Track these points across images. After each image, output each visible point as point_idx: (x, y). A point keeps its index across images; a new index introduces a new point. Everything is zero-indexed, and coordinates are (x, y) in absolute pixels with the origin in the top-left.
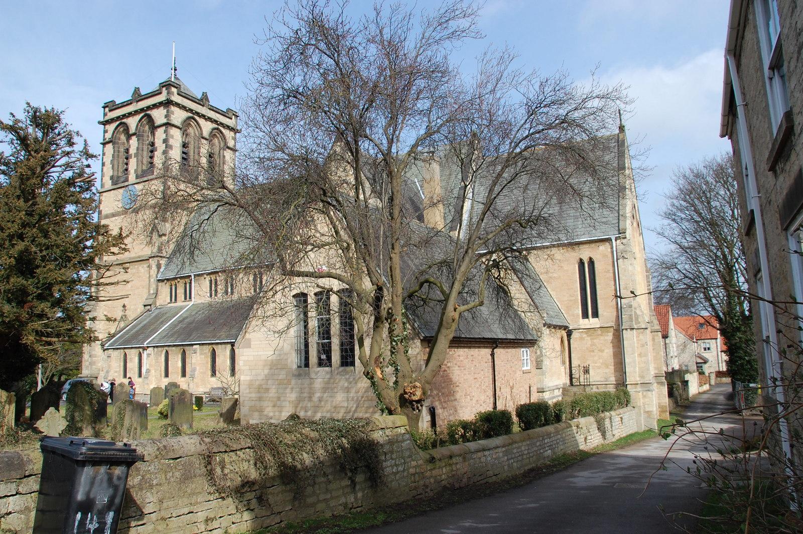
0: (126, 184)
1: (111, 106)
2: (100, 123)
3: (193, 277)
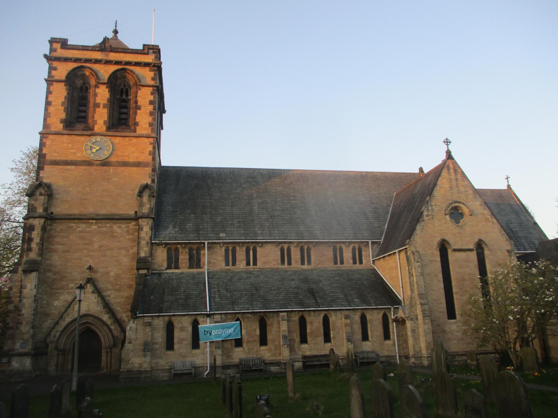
0: (89, 132)
1: (64, 43)
2: (45, 56)
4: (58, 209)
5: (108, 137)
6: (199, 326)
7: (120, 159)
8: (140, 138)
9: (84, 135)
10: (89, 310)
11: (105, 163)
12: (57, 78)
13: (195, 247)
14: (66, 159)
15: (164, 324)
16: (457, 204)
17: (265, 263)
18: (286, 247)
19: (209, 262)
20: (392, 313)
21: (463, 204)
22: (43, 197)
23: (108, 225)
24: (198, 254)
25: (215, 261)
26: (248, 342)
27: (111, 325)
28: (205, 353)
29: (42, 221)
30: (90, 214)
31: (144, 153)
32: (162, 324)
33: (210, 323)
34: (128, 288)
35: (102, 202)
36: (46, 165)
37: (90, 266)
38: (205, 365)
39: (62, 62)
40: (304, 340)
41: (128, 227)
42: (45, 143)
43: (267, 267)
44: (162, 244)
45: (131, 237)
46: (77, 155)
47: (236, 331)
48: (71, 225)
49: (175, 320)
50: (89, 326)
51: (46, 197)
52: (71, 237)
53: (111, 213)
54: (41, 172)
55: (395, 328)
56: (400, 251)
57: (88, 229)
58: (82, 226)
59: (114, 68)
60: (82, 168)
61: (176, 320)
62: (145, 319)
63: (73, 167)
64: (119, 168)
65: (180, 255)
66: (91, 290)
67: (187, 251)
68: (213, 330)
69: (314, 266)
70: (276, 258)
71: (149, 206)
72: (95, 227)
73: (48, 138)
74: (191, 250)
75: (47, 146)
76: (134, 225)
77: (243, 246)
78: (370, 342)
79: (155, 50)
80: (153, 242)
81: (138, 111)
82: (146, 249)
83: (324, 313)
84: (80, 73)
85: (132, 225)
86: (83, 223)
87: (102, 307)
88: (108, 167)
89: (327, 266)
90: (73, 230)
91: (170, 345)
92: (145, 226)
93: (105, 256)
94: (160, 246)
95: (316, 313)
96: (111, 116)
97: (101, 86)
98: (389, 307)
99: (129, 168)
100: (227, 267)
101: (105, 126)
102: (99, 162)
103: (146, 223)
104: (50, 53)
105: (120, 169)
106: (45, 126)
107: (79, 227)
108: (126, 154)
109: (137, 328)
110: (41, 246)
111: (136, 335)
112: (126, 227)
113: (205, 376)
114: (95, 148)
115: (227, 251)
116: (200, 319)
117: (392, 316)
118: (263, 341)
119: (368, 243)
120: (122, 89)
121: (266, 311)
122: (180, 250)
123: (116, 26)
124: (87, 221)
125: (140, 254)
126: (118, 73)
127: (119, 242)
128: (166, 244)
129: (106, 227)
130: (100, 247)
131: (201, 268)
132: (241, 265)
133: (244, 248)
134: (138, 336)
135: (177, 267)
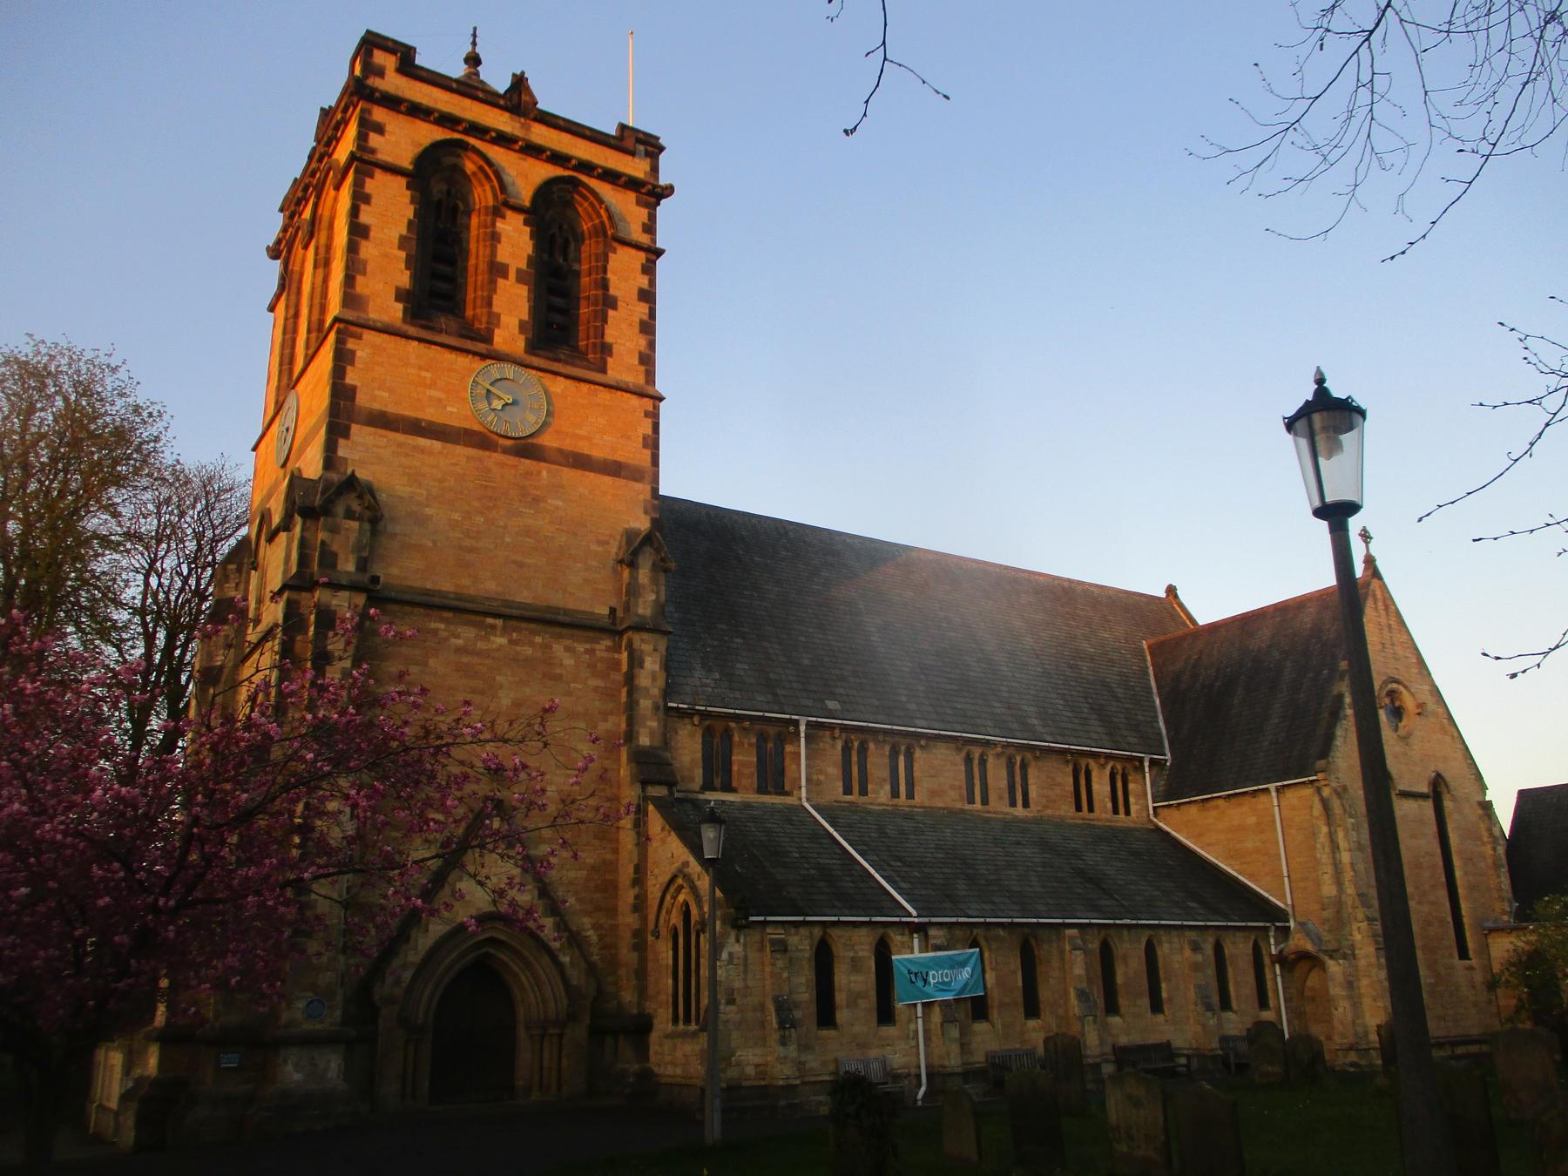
0: (481, 347)
3: (802, 728)
4: (395, 571)
5: (534, 372)
6: (894, 957)
7: (568, 445)
8: (619, 393)
9: (468, 352)
11: (526, 449)
13: (772, 731)
14: (415, 415)
15: (811, 949)
16: (1394, 686)
17: (933, 793)
18: (977, 752)
19: (808, 780)
20: (1272, 941)
21: (1406, 687)
22: (355, 525)
23: (538, 639)
24: (781, 754)
25: (822, 778)
27: (560, 950)
28: (911, 1035)
29: (361, 600)
30: (488, 599)
31: (629, 438)
32: (808, 948)
33: (921, 952)
34: (595, 838)
35: (521, 565)
36: (357, 423)
38: (913, 1071)
39: (399, 112)
40: (1112, 1007)
42: (353, 353)
43: (940, 805)
44: (694, 714)
45: (599, 683)
46: (449, 409)
47: (975, 977)
48: (433, 625)
49: (838, 938)
50: (492, 951)
51: (367, 526)
52: (431, 662)
53: (545, 604)
54: (341, 442)
55: (1279, 979)
56: (1284, 786)
57: (480, 645)
58: (466, 634)
60: (461, 450)
61: (840, 937)
62: (769, 930)
63: (437, 445)
64: (565, 469)
65: (735, 751)
67: (754, 740)
68: (933, 969)
69: (1038, 811)
70: (957, 783)
71: (653, 597)
72: (501, 641)
73: (360, 338)
74: (763, 738)
75: (358, 364)
76: (608, 649)
77: (884, 741)
78: (1235, 1012)
79: (650, 149)
80: (670, 704)
81: (611, 313)
82: (654, 724)
83: (1146, 934)
84: (448, 160)
85: (604, 648)
86: (468, 623)
87: (536, 893)
88: (535, 463)
89: (1062, 813)
90: (439, 643)
91: (826, 1014)
92: (650, 655)
94: (687, 721)
95: (1133, 931)
97: (509, 213)
98: (1268, 924)
99: (593, 474)
100: (848, 798)
101: (523, 337)
102: (509, 443)
103: (652, 647)
105: (569, 475)
107: (457, 637)
108: (583, 432)
109: (746, 958)
111: (745, 979)
112: (586, 651)
113: (920, 1103)
114: (500, 398)
115: (847, 749)
116: (896, 938)
117: (1273, 947)
118: (1032, 1007)
119: (1141, 760)
121: (1038, 923)
122: (736, 738)
123: (474, 44)
124: (479, 618)
125: (638, 739)
126: (555, 189)
128: (704, 715)
129: (532, 644)
131: (788, 794)
132: (880, 795)
133: (887, 748)
134: (750, 983)
135: (728, 788)
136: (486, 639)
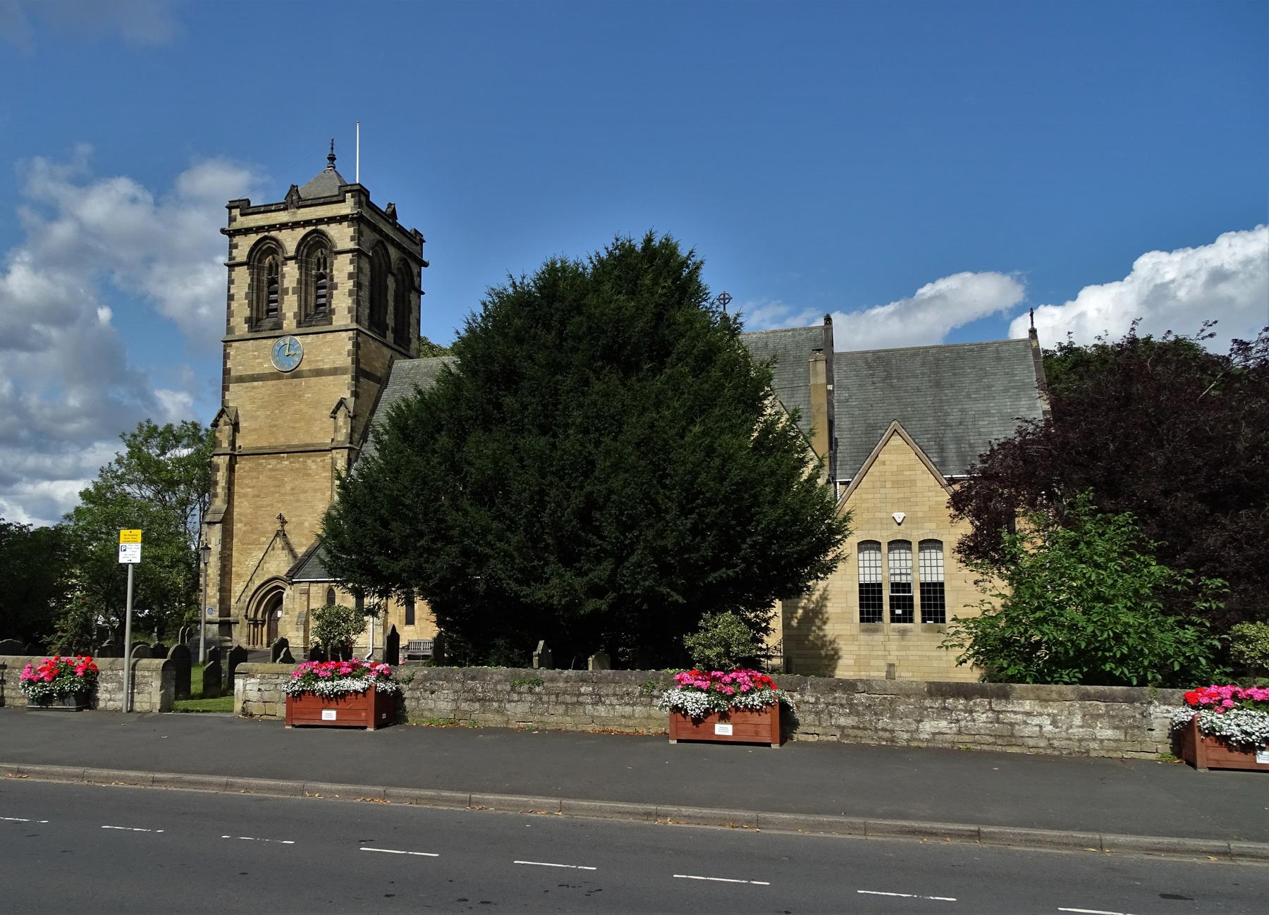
0: (277, 333)
2: (223, 231)
7: (313, 367)
10: (279, 572)
12: (238, 260)
22: (227, 427)
23: (301, 459)
26: (420, 619)
35: (294, 428)
37: (280, 515)
41: (324, 460)
51: (231, 427)
54: (227, 393)
57: (279, 466)
58: (272, 462)
59: (301, 232)
60: (270, 383)
66: (280, 546)
71: (345, 431)
72: (286, 463)
81: (335, 292)
93: (298, 501)
96: (303, 303)
97: (289, 262)
104: (229, 225)
106: (230, 330)
110: (227, 491)
112: (321, 461)
120: (319, 260)
123: (332, 148)
127: (313, 481)
130: (293, 489)
136: (280, 463)
